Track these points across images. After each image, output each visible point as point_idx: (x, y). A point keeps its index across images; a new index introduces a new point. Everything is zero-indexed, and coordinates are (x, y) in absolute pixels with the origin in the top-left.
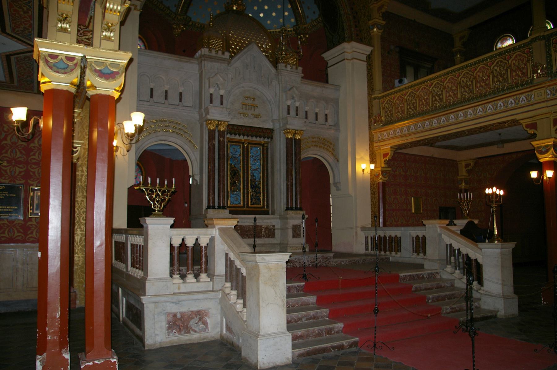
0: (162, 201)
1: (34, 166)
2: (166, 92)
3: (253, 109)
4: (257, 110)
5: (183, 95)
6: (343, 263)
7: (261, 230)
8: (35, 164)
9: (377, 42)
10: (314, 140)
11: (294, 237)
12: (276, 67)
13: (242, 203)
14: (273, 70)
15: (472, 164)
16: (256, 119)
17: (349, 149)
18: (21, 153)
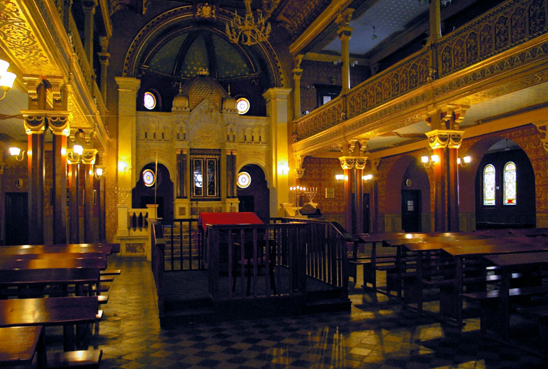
2: (155, 134)
9: (298, 84)
14: (220, 114)
15: (378, 162)
16: (209, 144)
17: (274, 158)
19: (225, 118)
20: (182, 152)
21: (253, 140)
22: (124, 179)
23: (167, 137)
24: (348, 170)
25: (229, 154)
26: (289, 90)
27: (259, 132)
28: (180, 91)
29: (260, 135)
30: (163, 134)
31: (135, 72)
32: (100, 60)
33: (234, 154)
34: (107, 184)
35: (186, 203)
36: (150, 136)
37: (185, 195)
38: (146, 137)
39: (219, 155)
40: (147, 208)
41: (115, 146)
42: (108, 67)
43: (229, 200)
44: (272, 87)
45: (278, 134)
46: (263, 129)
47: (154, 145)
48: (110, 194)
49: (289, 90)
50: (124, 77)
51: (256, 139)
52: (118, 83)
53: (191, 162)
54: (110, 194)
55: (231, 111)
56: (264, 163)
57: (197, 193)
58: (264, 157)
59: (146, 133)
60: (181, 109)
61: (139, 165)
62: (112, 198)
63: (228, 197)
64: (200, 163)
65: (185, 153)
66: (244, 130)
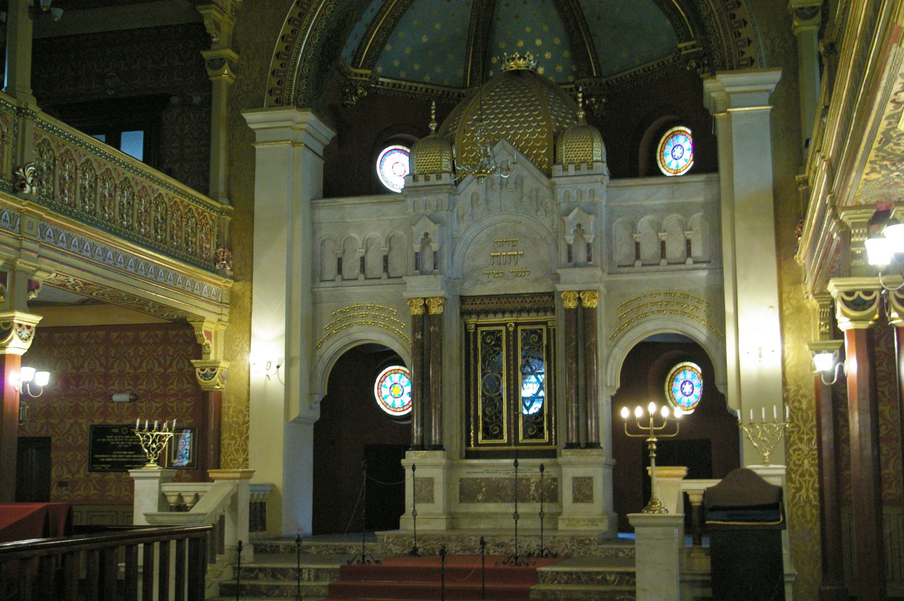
0: (159, 448)
1: (172, 399)
2: (363, 259)
3: (513, 263)
4: (521, 262)
5: (389, 260)
6: (621, 554)
7: (528, 486)
8: (175, 395)
10: (658, 299)
11: (576, 500)
12: (549, 176)
13: (505, 437)
14: (544, 179)
16: (519, 279)
18: (158, 383)
19: (560, 193)
20: (426, 307)
21: (663, 255)
22: (264, 393)
23: (398, 264)
24: (857, 331)
25: (572, 305)
26: (776, 76)
27: (685, 227)
28: (433, 126)
29: (689, 234)
30: (386, 259)
31: (298, 91)
32: (210, 72)
33: (587, 304)
34: (224, 410)
35: (436, 466)
36: (351, 266)
37: (435, 438)
38: (340, 270)
39: (553, 310)
40: (212, 480)
41: (247, 300)
42: (231, 88)
43: (567, 456)
44: (713, 74)
45: (740, 226)
46: (697, 217)
47: (359, 293)
48: (233, 438)
49: (776, 76)
50: (270, 107)
51: (675, 249)
52: (252, 126)
53: (468, 338)
54: (233, 438)
55: (577, 168)
56: (704, 330)
57: (487, 434)
58: (703, 307)
59: (340, 262)
60: (427, 179)
61: (318, 353)
62: (237, 451)
63: (569, 446)
64: (499, 340)
65: (434, 310)
66: (633, 226)
